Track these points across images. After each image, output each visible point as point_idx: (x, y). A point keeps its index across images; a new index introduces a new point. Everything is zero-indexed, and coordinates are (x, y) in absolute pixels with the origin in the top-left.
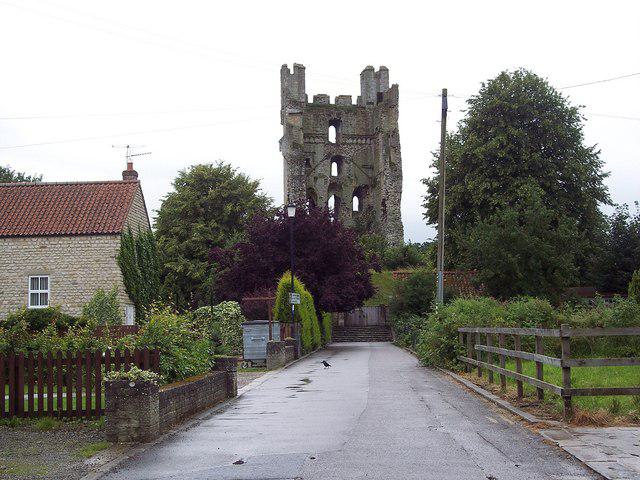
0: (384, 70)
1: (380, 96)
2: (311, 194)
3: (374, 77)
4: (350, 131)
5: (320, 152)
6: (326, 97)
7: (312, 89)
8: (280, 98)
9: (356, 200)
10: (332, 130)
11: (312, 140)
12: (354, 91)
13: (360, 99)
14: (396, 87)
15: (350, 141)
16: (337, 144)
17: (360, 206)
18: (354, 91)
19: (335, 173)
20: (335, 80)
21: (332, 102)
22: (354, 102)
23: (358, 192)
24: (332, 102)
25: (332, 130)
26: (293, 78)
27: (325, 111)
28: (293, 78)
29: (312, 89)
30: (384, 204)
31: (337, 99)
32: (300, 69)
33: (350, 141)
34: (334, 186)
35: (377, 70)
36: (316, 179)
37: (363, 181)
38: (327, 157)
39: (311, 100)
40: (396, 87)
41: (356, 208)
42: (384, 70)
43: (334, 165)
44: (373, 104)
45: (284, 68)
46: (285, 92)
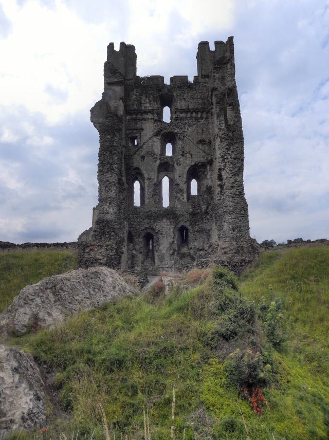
7: (144, 68)
8: (104, 81)
9: (194, 183)
12: (191, 71)
15: (183, 115)
17: (199, 190)
18: (191, 71)
19: (169, 152)
20: (164, 57)
21: (167, 82)
22: (191, 80)
23: (195, 172)
24: (167, 82)
25: (167, 111)
26: (120, 61)
27: (159, 91)
28: (120, 61)
29: (144, 68)
30: (220, 177)
31: (172, 79)
36: (143, 157)
37: (200, 158)
38: (156, 134)
41: (194, 191)
43: (169, 147)
45: (111, 46)
46: (110, 69)
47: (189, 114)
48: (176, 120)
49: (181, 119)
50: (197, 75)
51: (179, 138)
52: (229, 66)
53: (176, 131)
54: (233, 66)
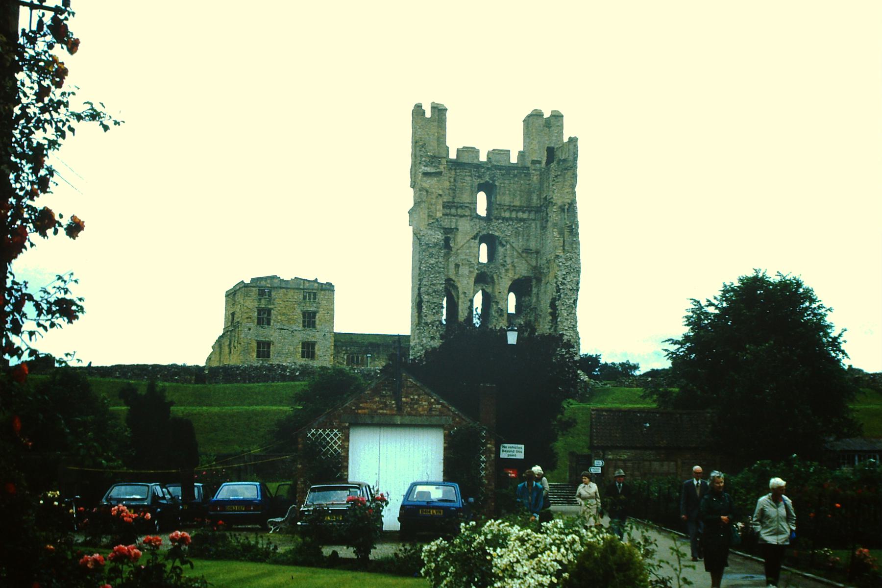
0: (557, 117)
1: (551, 152)
2: (450, 289)
3: (543, 126)
4: (506, 200)
5: (465, 228)
6: (474, 151)
7: (455, 141)
9: (512, 298)
10: (482, 199)
11: (453, 211)
12: (513, 143)
13: (521, 155)
14: (573, 141)
16: (488, 219)
18: (513, 143)
19: (483, 258)
20: (488, 130)
21: (483, 158)
22: (514, 159)
29: (455, 141)
30: (553, 305)
32: (439, 112)
33: (507, 215)
34: (483, 278)
35: (547, 115)
37: (523, 270)
38: (474, 238)
39: (453, 155)
40: (573, 141)
42: (557, 117)
43: (484, 248)
44: (540, 162)
45: (418, 111)
46: (418, 145)
47: (514, 215)
48: (498, 220)
49: (504, 219)
50: (522, 149)
51: (501, 243)
52: (570, 173)
53: (496, 234)
54: (575, 176)
